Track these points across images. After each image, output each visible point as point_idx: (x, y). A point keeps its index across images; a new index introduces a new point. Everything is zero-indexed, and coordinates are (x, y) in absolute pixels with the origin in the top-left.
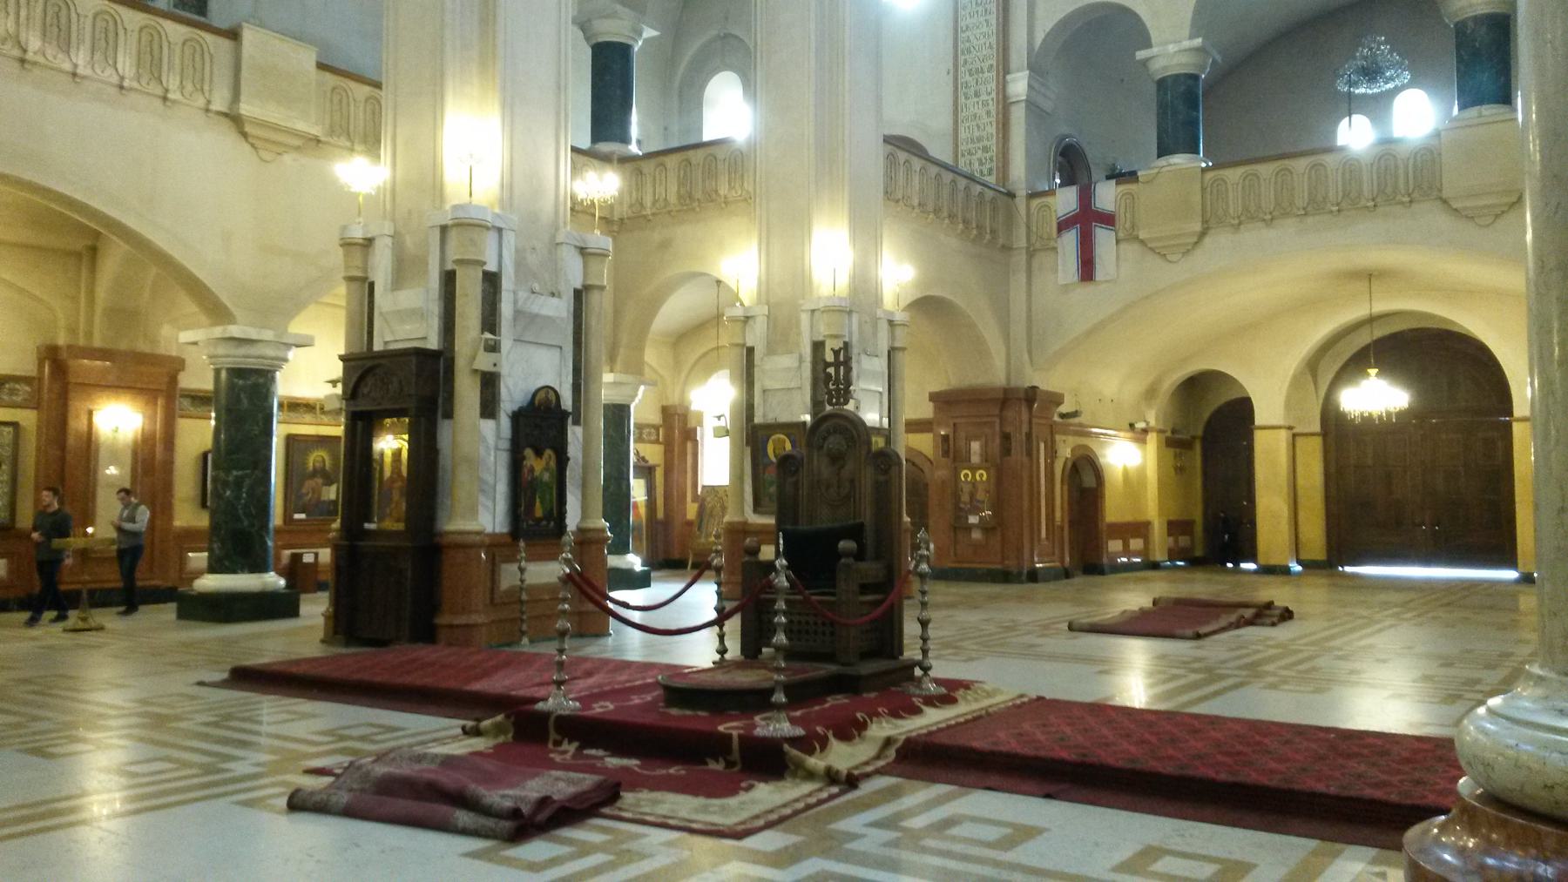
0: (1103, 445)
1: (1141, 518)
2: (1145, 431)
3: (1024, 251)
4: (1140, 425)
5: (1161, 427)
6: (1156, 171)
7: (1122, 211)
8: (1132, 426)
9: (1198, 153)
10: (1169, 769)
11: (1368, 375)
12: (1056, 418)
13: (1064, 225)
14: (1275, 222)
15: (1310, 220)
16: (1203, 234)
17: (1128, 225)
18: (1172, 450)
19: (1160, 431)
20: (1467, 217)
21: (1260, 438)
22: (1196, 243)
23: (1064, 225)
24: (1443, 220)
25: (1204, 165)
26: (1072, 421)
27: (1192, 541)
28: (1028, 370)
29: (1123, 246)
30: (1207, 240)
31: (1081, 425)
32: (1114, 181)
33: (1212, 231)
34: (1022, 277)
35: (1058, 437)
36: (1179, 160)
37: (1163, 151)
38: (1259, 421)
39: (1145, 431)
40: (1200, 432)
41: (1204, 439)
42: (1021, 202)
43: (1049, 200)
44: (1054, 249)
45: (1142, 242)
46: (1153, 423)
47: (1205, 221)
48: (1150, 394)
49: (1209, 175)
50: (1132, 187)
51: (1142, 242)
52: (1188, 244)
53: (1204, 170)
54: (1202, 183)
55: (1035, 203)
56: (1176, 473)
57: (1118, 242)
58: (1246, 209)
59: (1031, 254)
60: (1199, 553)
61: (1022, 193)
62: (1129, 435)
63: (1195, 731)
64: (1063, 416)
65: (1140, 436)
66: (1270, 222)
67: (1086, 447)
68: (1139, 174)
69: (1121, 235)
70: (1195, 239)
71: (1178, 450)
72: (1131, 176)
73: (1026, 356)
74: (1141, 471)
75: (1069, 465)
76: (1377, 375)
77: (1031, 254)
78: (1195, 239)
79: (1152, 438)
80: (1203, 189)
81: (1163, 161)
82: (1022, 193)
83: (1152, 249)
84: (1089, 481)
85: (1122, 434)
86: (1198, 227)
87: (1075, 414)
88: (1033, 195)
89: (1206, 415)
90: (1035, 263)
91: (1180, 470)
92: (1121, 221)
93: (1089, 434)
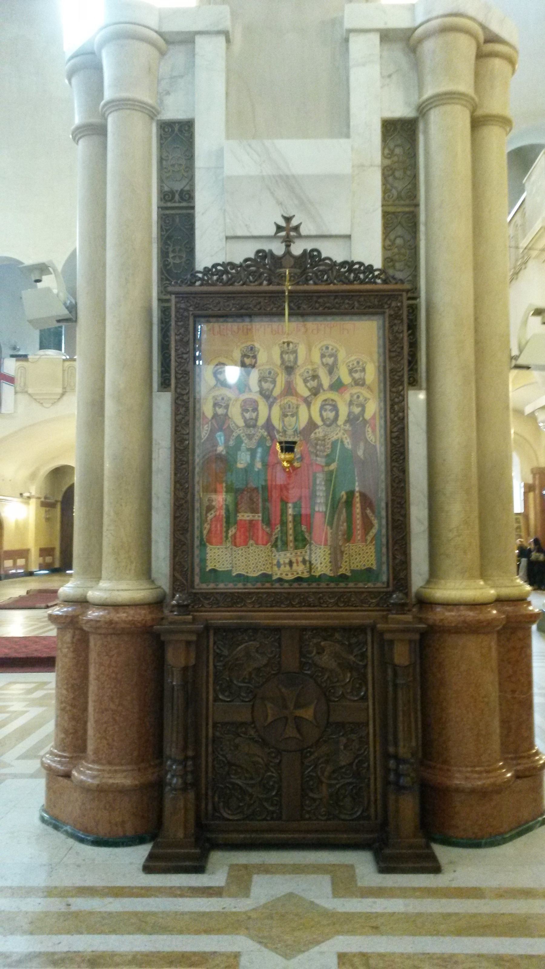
1: (25, 547)
4: (26, 494)
5: (38, 496)
6: (38, 357)
7: (19, 375)
8: (21, 494)
9: (60, 349)
10: (22, 655)
16: (63, 394)
17: (22, 384)
18: (44, 509)
19: (38, 498)
22: (59, 399)
25: (64, 358)
27: (53, 559)
29: (19, 396)
30: (65, 398)
32: (14, 359)
33: (67, 394)
36: (51, 353)
37: (42, 346)
39: (29, 498)
40: (60, 498)
41: (62, 503)
45: (30, 395)
46: (33, 493)
47: (64, 388)
48: (33, 476)
49: (67, 364)
51: (30, 395)
52: (55, 399)
53: (64, 360)
54: (63, 367)
56: (46, 521)
57: (16, 393)
60: (57, 565)
62: (20, 500)
63: (36, 642)
68: (29, 357)
70: (58, 397)
71: (47, 509)
72: (24, 357)
79: (33, 502)
81: (42, 352)
83: (35, 399)
86: (60, 390)
91: (48, 519)
92: (19, 381)
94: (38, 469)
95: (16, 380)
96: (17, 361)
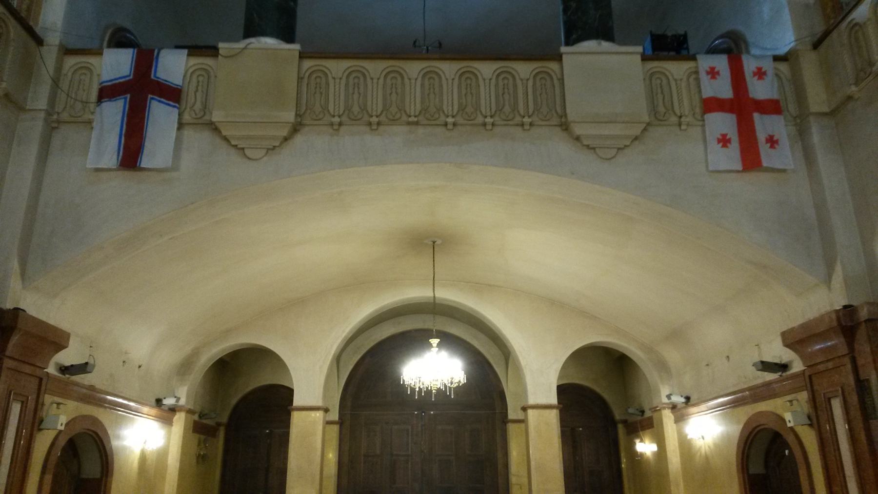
0: (120, 422)
2: (173, 410)
3: (42, 115)
4: (169, 401)
5: (191, 406)
8: (159, 402)
11: (431, 346)
12: (51, 370)
13: (108, 92)
14: (381, 128)
15: (421, 130)
16: (296, 129)
17: (198, 106)
18: (197, 436)
19: (190, 412)
20: (588, 146)
21: (297, 418)
22: (286, 139)
23: (108, 92)
24: (562, 147)
26: (77, 378)
28: (15, 283)
29: (187, 133)
30: (299, 139)
31: (92, 388)
32: (186, 51)
33: (306, 129)
34: (34, 149)
35: (48, 399)
37: (251, 31)
38: (297, 401)
39: (173, 410)
40: (224, 419)
41: (229, 426)
42: (50, 55)
43: (92, 60)
44: (90, 122)
46: (182, 402)
48: (184, 368)
50: (209, 61)
55: (71, 61)
56: (198, 462)
57: (181, 126)
58: (348, 108)
59: (52, 125)
61: (53, 39)
62: (154, 411)
64: (64, 370)
65: (166, 414)
66: (373, 126)
67: (95, 421)
69: (187, 117)
71: (203, 437)
72: (212, 51)
73: (15, 265)
74: (162, 454)
75: (62, 442)
76: (439, 345)
77: (52, 125)
78: (285, 132)
79: (180, 420)
80: (300, 79)
82: (53, 39)
83: (226, 139)
84: (91, 469)
85: (146, 409)
87: (83, 368)
88: (67, 51)
89: (234, 401)
90: (56, 140)
91: (202, 459)
92: (193, 99)
93: (101, 403)
94: (195, 354)
95: (184, 96)
96: (189, 55)
